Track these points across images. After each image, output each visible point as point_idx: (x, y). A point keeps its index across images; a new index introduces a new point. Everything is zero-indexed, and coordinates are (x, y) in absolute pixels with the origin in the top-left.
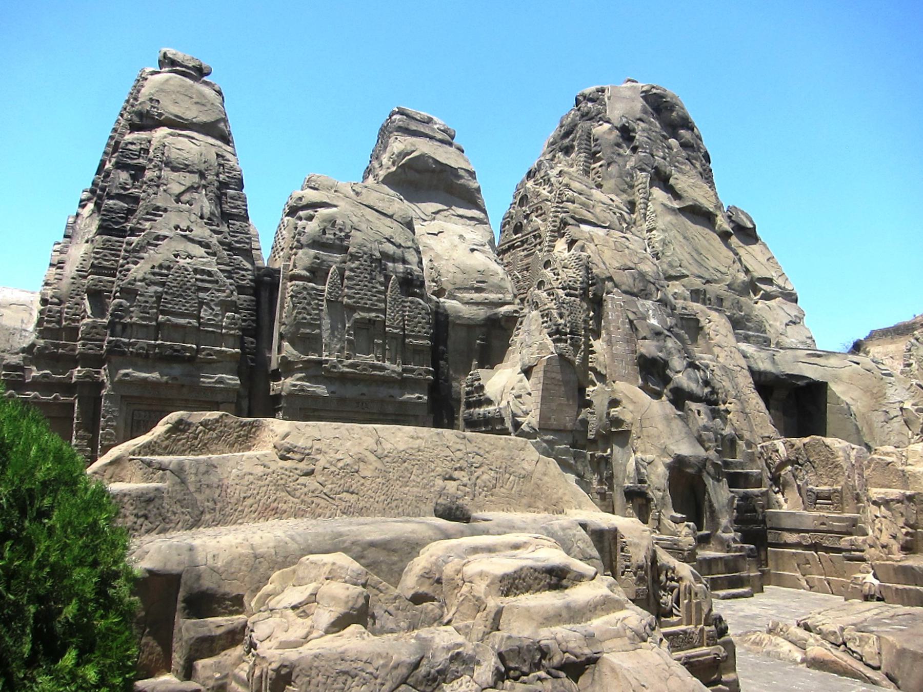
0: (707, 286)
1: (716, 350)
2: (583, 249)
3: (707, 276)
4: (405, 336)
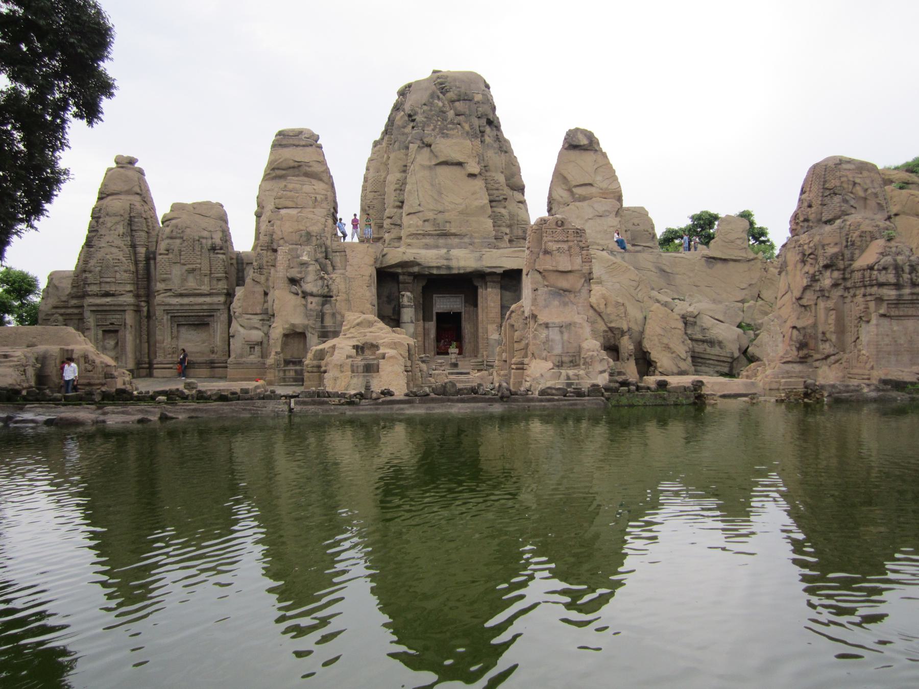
0: (440, 216)
1: (348, 268)
2: (273, 225)
3: (441, 208)
4: (211, 273)
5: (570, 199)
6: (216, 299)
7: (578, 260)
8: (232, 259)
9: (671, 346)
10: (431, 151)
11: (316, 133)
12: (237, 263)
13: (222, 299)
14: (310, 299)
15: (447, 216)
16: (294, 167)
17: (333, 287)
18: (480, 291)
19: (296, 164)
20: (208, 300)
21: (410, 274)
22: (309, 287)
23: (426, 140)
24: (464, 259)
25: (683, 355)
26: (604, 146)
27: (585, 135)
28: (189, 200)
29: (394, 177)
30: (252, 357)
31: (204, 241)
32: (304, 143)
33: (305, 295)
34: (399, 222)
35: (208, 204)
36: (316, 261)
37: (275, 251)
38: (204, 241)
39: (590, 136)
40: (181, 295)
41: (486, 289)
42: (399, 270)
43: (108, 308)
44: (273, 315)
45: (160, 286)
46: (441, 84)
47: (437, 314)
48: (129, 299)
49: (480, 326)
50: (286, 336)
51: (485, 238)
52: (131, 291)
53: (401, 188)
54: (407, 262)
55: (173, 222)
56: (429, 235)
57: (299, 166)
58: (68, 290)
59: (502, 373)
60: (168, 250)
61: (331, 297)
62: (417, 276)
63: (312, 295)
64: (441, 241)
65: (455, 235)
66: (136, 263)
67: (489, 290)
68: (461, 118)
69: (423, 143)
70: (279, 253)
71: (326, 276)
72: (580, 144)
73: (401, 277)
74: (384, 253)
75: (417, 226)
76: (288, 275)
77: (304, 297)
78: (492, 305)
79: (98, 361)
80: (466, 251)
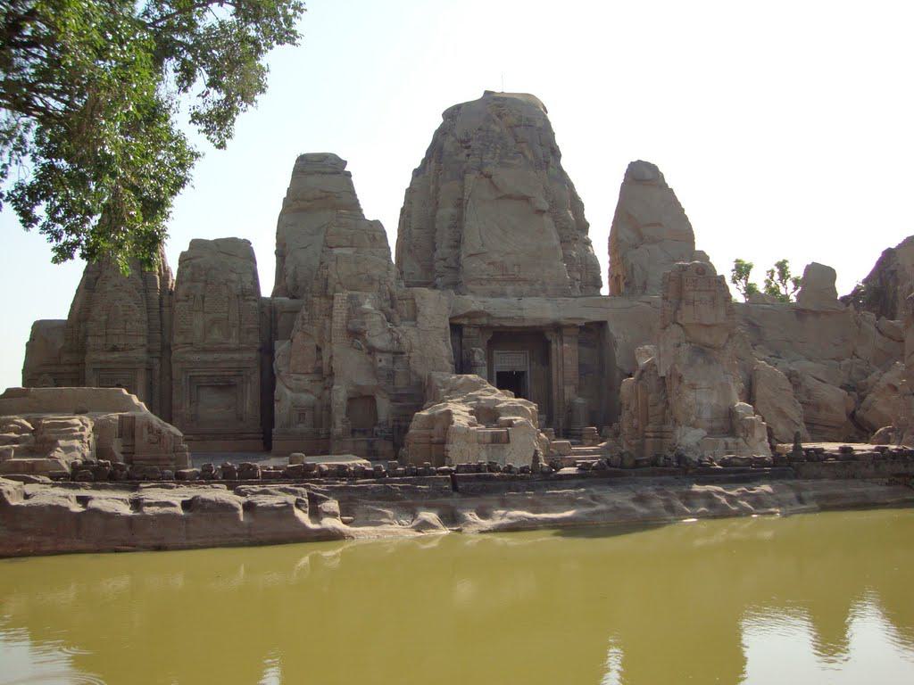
6: (247, 355)
7: (722, 313)
8: (262, 306)
9: (786, 410)
10: (492, 182)
12: (271, 312)
13: (253, 355)
14: (379, 356)
16: (321, 198)
17: (404, 341)
18: (554, 346)
19: (324, 194)
20: (237, 356)
22: (378, 343)
23: (486, 170)
24: (538, 310)
25: (797, 420)
26: (671, 181)
28: (211, 235)
29: (447, 211)
30: (301, 425)
31: (233, 285)
33: (372, 351)
34: (454, 265)
35: (233, 241)
36: (382, 310)
37: (333, 298)
38: (233, 285)
39: (653, 168)
40: (205, 350)
41: (562, 344)
42: (465, 322)
43: (112, 366)
44: (332, 374)
45: (178, 339)
46: (499, 106)
47: (498, 373)
48: (141, 354)
49: (555, 387)
50: (350, 400)
52: (143, 345)
53: (458, 223)
54: (475, 312)
55: (194, 261)
56: (494, 280)
57: (327, 197)
58: (60, 344)
59: (634, 442)
60: (187, 296)
61: (402, 353)
62: (482, 328)
63: (382, 352)
64: (509, 289)
65: (525, 280)
66: (149, 310)
67: (565, 345)
68: (523, 145)
69: (482, 173)
70: (335, 301)
71: (395, 329)
72: (643, 182)
73: (466, 331)
76: (350, 326)
77: (369, 353)
79: (164, 430)
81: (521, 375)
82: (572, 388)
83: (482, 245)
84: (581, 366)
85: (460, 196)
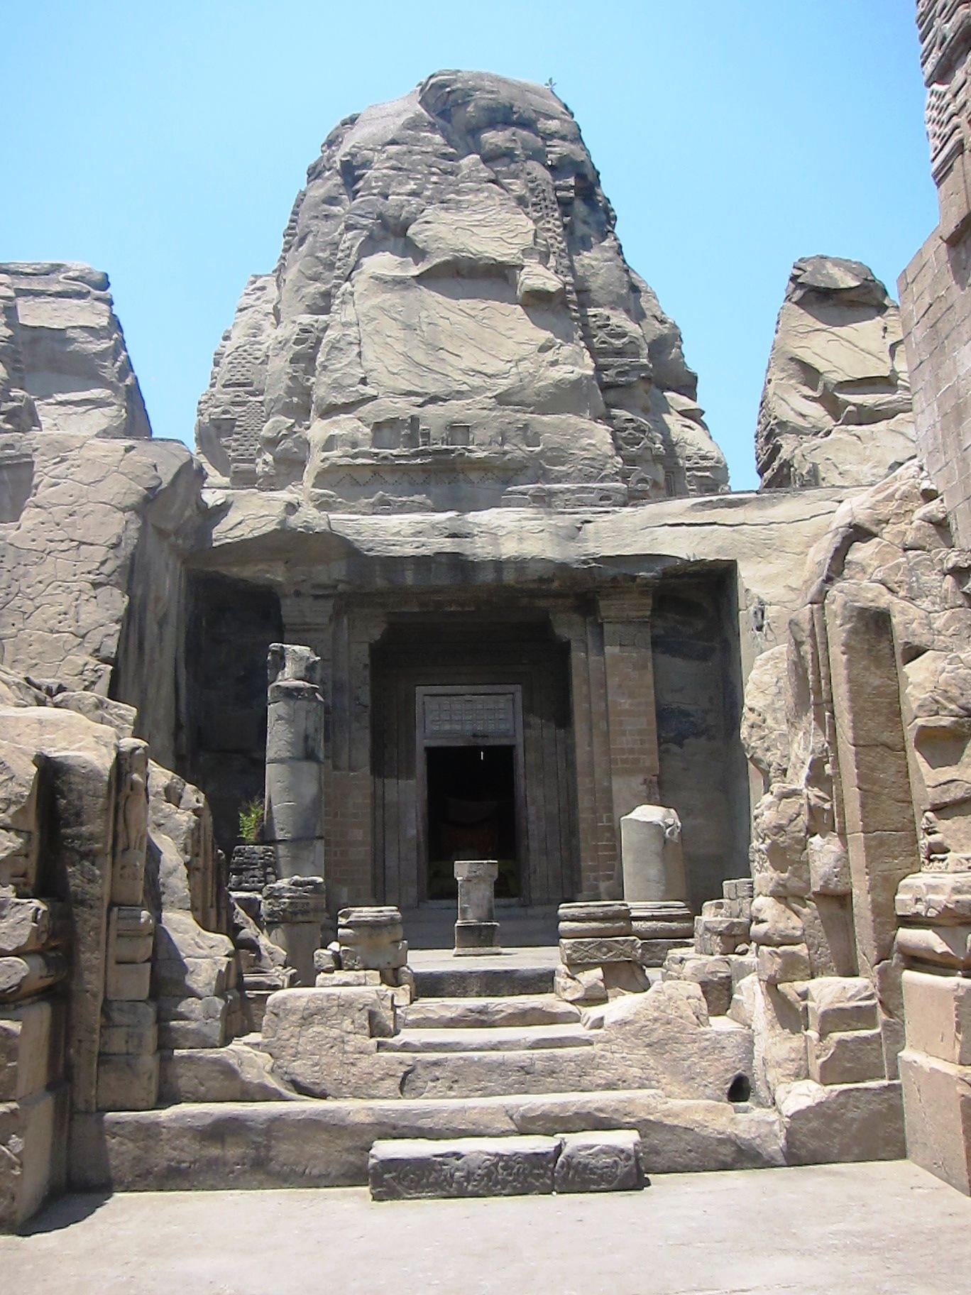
3: (433, 389)
5: (828, 422)
11: (99, 268)
15: (454, 410)
18: (577, 656)
21: (322, 593)
27: (849, 270)
32: (58, 288)
41: (601, 651)
42: (277, 574)
47: (429, 750)
49: (583, 782)
51: (589, 478)
74: (211, 498)
75: (354, 445)
78: (625, 703)
80: (528, 512)
81: (502, 757)
82: (636, 783)
83: (363, 381)
84: (663, 715)
85: (323, 288)
